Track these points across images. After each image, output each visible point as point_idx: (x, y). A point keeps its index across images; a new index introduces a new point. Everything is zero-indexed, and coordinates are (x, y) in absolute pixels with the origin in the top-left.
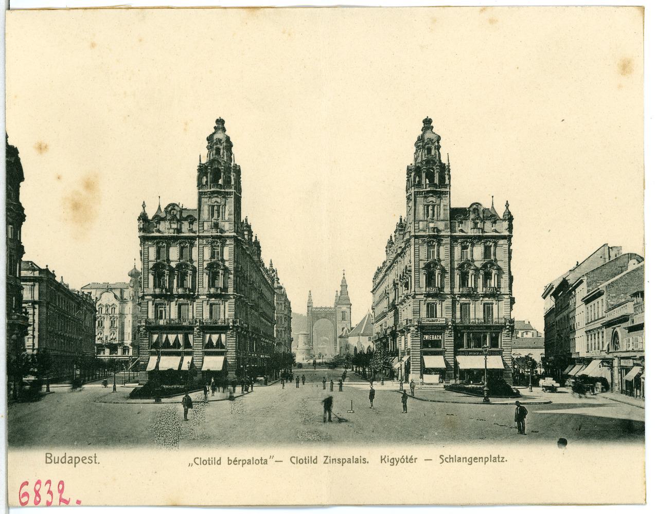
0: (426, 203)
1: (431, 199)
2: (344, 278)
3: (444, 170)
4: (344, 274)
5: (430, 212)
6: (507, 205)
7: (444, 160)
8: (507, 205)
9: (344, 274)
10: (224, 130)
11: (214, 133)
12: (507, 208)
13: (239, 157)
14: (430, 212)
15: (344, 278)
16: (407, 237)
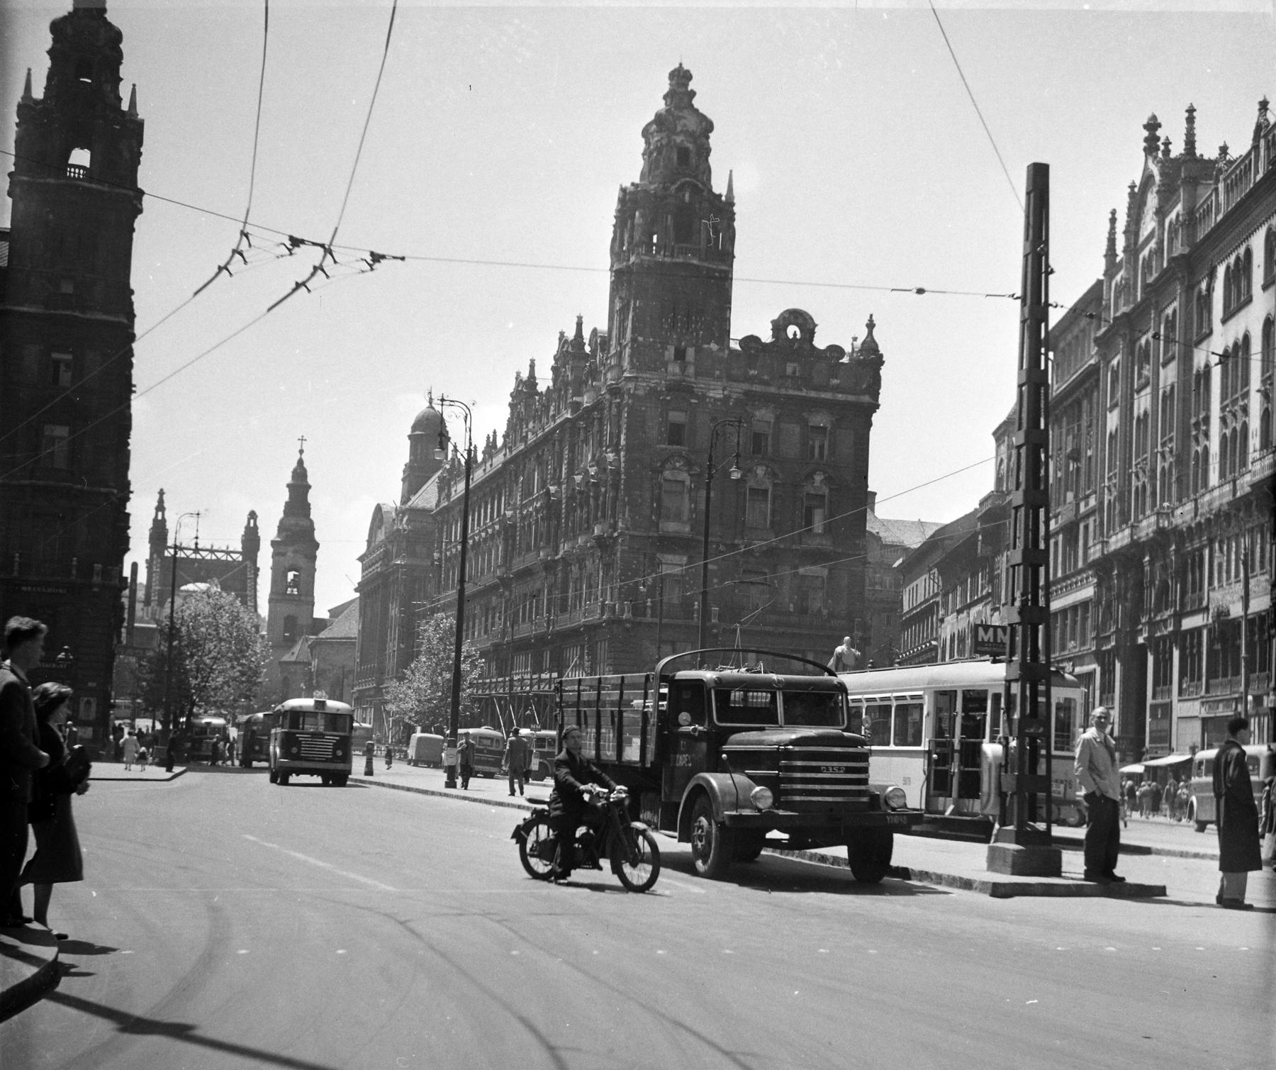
2: (301, 462)
4: (301, 452)
6: (871, 325)
7: (719, 187)
8: (871, 325)
9: (301, 452)
12: (870, 333)
15: (301, 462)
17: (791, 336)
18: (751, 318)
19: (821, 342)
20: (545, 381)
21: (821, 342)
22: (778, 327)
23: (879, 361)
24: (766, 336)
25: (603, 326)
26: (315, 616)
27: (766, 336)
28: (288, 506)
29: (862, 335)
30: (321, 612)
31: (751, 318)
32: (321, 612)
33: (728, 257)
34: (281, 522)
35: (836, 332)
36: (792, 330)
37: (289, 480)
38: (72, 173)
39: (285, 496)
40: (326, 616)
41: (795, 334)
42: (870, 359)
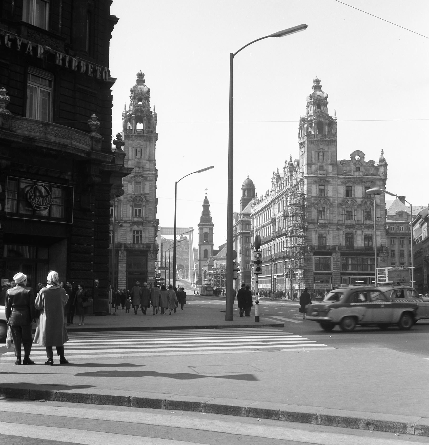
0: (317, 150)
1: (321, 147)
2: (206, 197)
3: (332, 123)
5: (321, 157)
6: (382, 153)
8: (382, 153)
9: (206, 194)
10: (144, 82)
11: (136, 85)
13: (156, 104)
14: (321, 157)
15: (206, 197)
16: (299, 176)
17: (357, 159)
18: (343, 154)
19: (367, 160)
20: (282, 175)
21: (367, 160)
22: (352, 156)
23: (386, 164)
24: (349, 159)
25: (298, 158)
26: (214, 249)
27: (349, 159)
28: (203, 212)
29: (379, 156)
30: (216, 248)
31: (343, 154)
32: (216, 248)
33: (335, 135)
34: (201, 218)
35: (372, 156)
36: (357, 157)
37: (203, 203)
38: (140, 132)
39: (202, 209)
40: (218, 249)
41: (358, 158)
42: (384, 163)
